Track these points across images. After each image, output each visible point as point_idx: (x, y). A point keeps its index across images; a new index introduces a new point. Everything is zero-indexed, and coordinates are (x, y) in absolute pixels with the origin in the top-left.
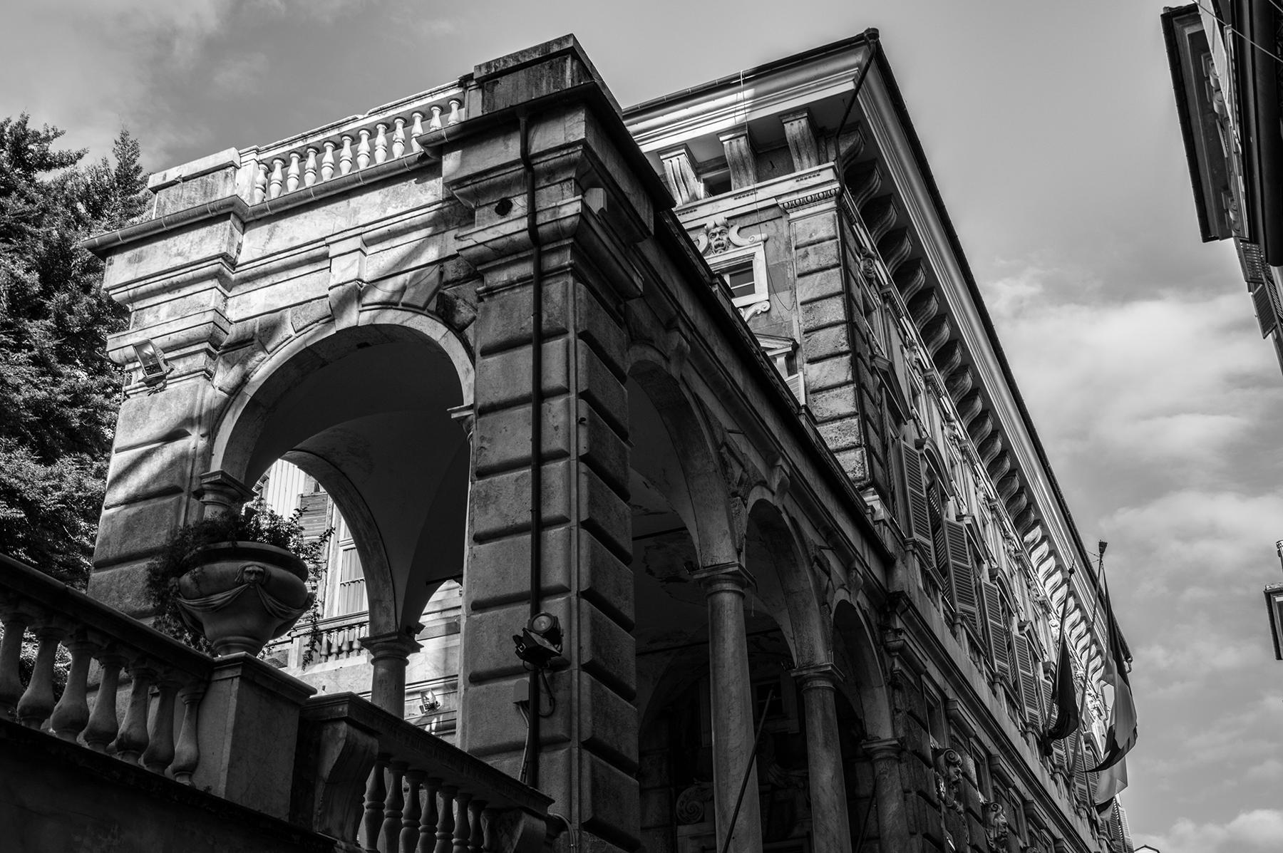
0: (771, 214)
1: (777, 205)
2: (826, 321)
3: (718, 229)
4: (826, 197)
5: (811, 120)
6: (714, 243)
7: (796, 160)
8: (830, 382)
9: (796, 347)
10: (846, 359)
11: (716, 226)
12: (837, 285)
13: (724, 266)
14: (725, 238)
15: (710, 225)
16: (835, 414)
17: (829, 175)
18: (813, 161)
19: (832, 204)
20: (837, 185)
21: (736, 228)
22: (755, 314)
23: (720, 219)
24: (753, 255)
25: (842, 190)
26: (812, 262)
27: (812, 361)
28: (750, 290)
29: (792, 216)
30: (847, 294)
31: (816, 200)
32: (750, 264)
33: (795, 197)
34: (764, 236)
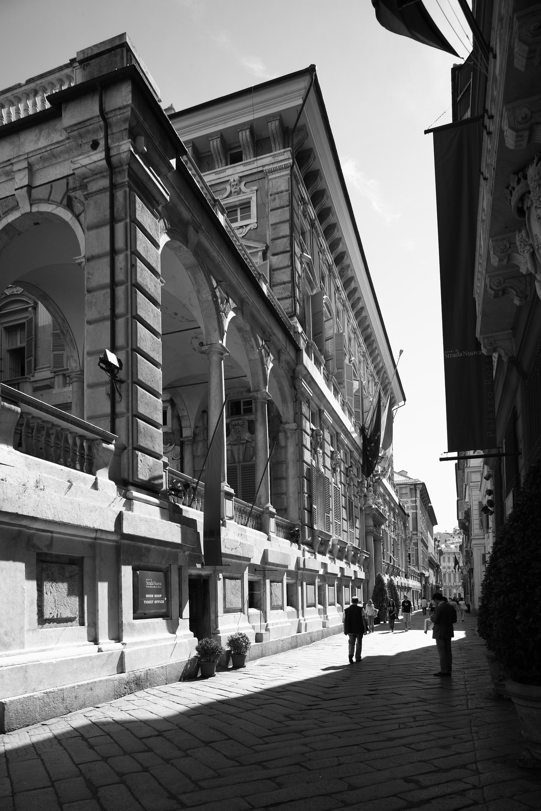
0: (260, 175)
1: (262, 171)
2: (281, 234)
3: (235, 183)
4: (286, 167)
5: (281, 121)
6: (233, 190)
7: (273, 145)
8: (281, 265)
9: (267, 247)
10: (289, 254)
11: (234, 181)
12: (287, 216)
13: (237, 203)
14: (238, 188)
15: (232, 180)
16: (282, 281)
17: (288, 155)
18: (281, 146)
19: (288, 172)
20: (291, 161)
21: (243, 183)
22: (250, 229)
23: (236, 177)
24: (251, 198)
25: (293, 163)
26: (277, 204)
27: (274, 255)
28: (249, 217)
29: (270, 177)
30: (291, 221)
31: (281, 169)
32: (249, 203)
33: (271, 166)
34: (255, 188)
